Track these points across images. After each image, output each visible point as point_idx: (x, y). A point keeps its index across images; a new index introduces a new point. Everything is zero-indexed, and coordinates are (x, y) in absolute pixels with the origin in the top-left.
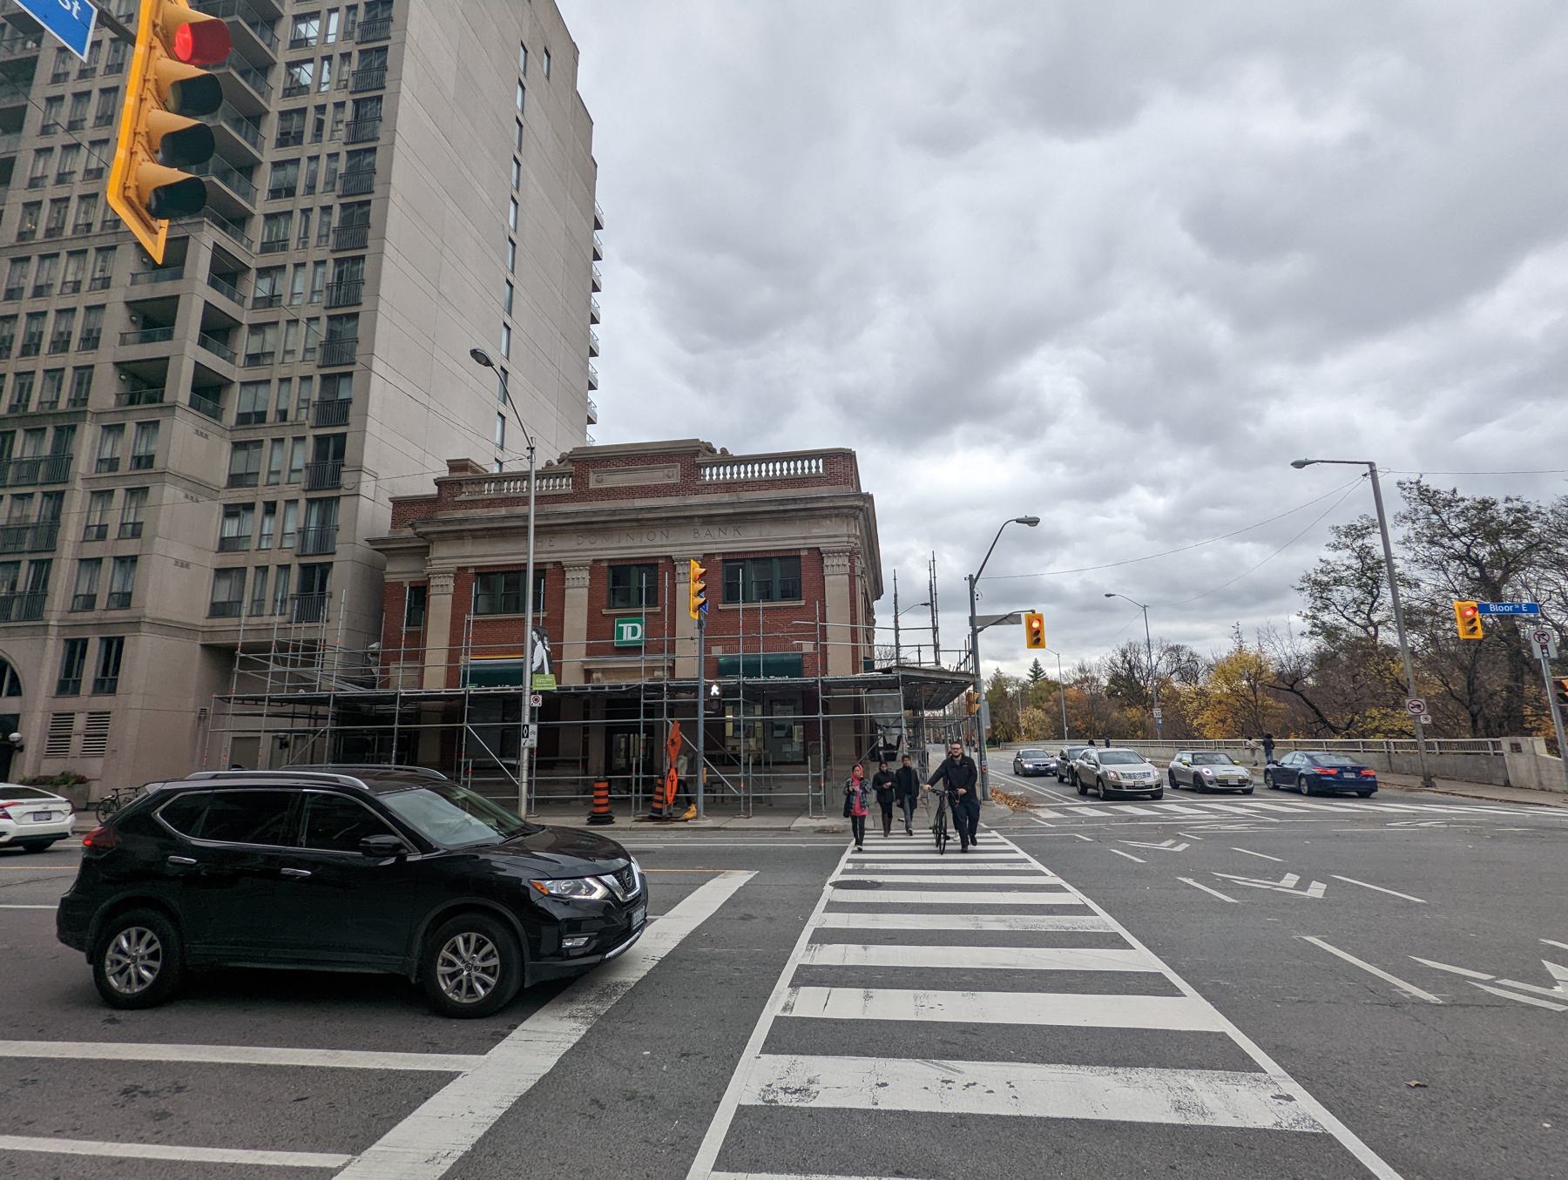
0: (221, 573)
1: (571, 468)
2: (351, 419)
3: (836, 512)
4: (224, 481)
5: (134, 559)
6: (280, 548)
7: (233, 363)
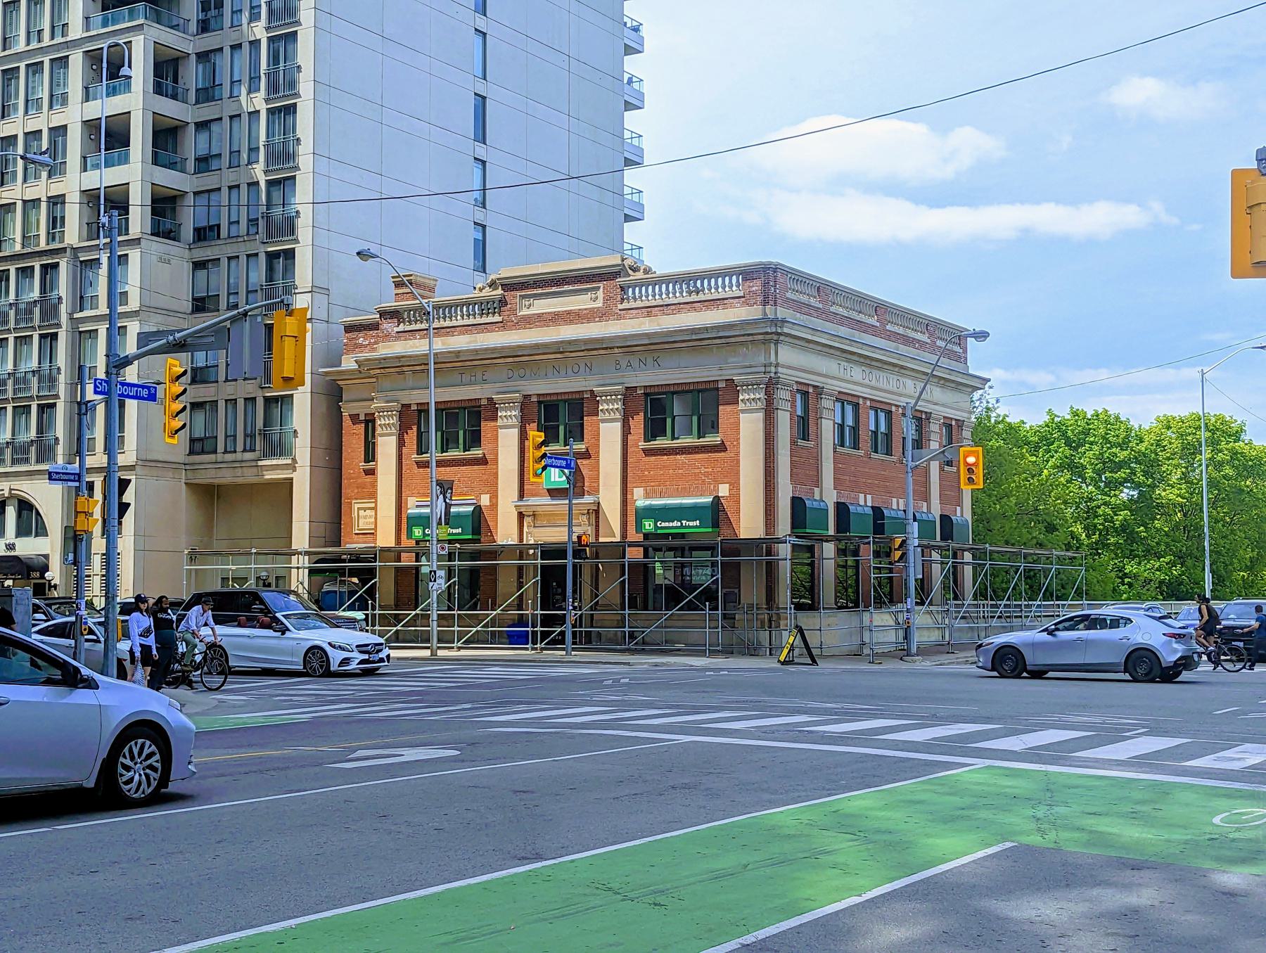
3: (750, 338)
4: (188, 307)
7: (183, 171)
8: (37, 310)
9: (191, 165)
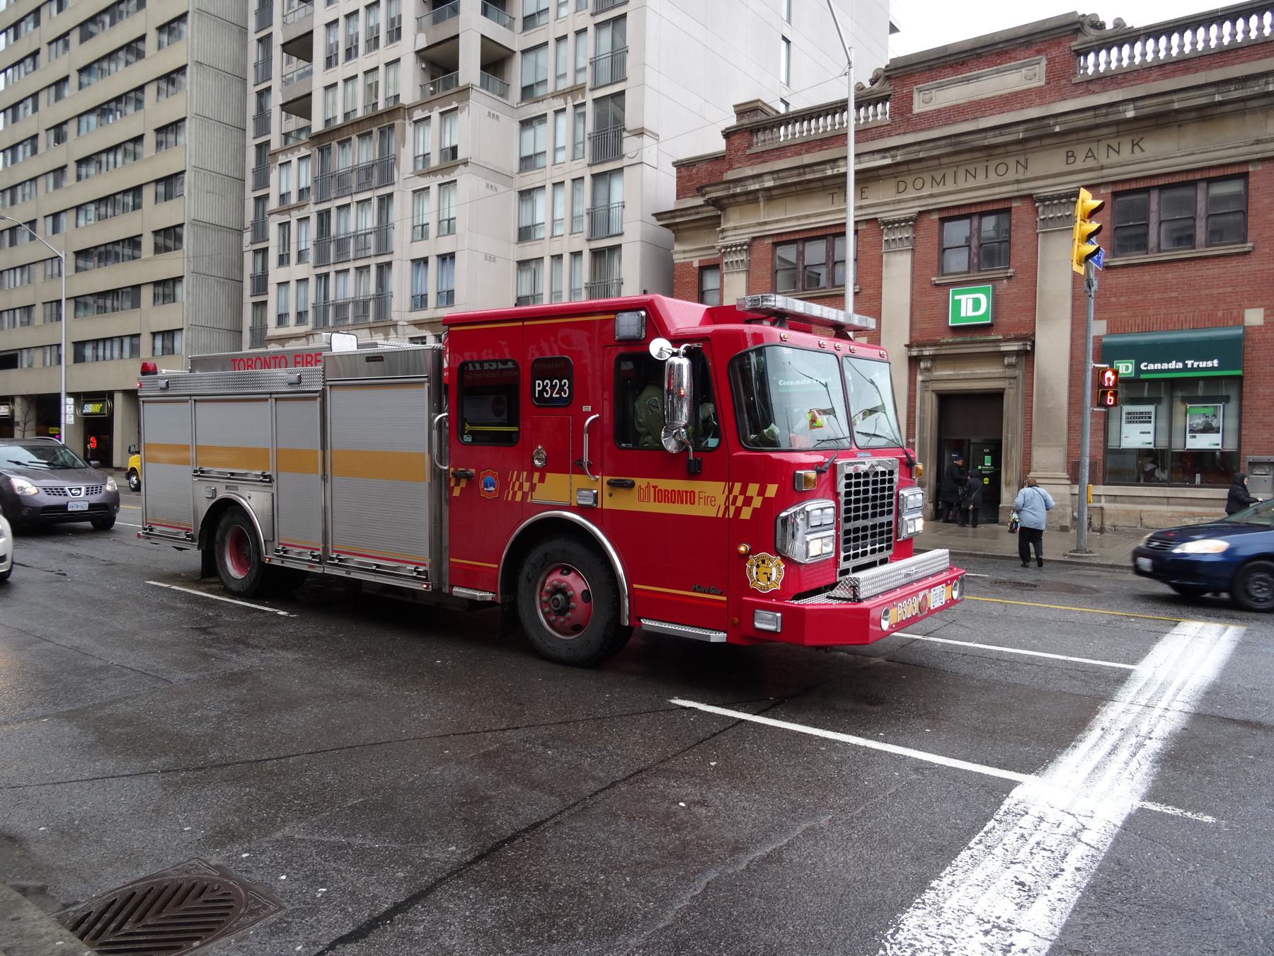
0: (522, 264)
1: (887, 89)
2: (630, 70)
5: (452, 256)
6: (572, 233)
8: (376, 172)
9: (518, 24)
